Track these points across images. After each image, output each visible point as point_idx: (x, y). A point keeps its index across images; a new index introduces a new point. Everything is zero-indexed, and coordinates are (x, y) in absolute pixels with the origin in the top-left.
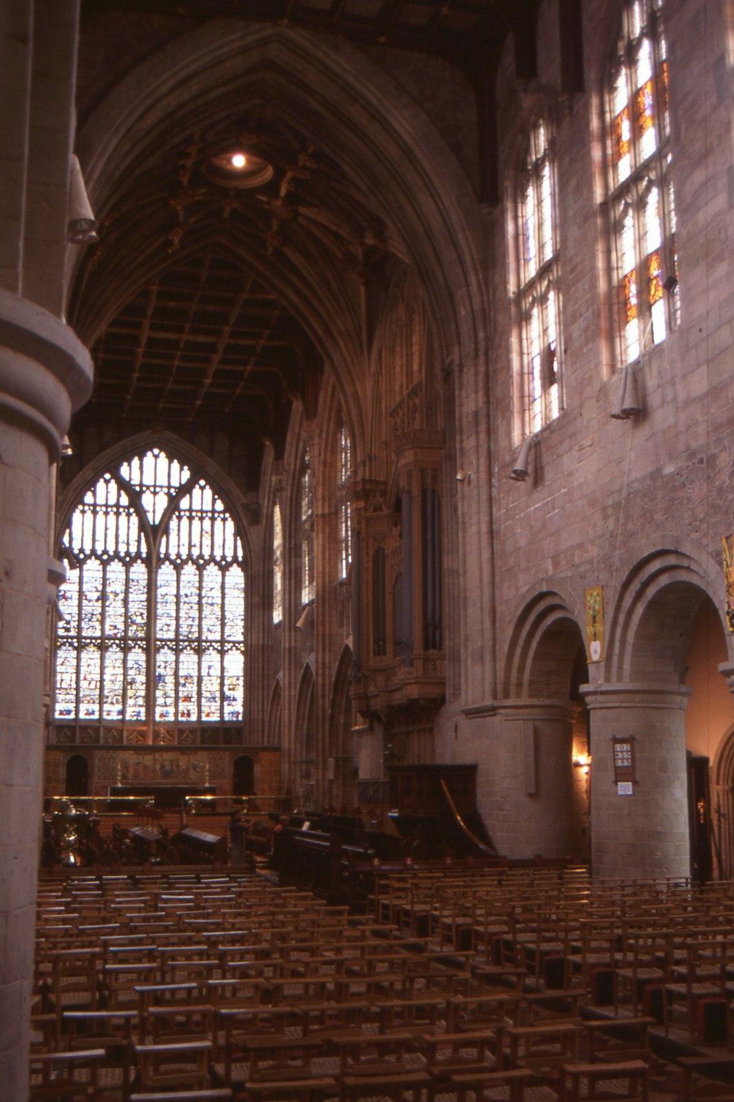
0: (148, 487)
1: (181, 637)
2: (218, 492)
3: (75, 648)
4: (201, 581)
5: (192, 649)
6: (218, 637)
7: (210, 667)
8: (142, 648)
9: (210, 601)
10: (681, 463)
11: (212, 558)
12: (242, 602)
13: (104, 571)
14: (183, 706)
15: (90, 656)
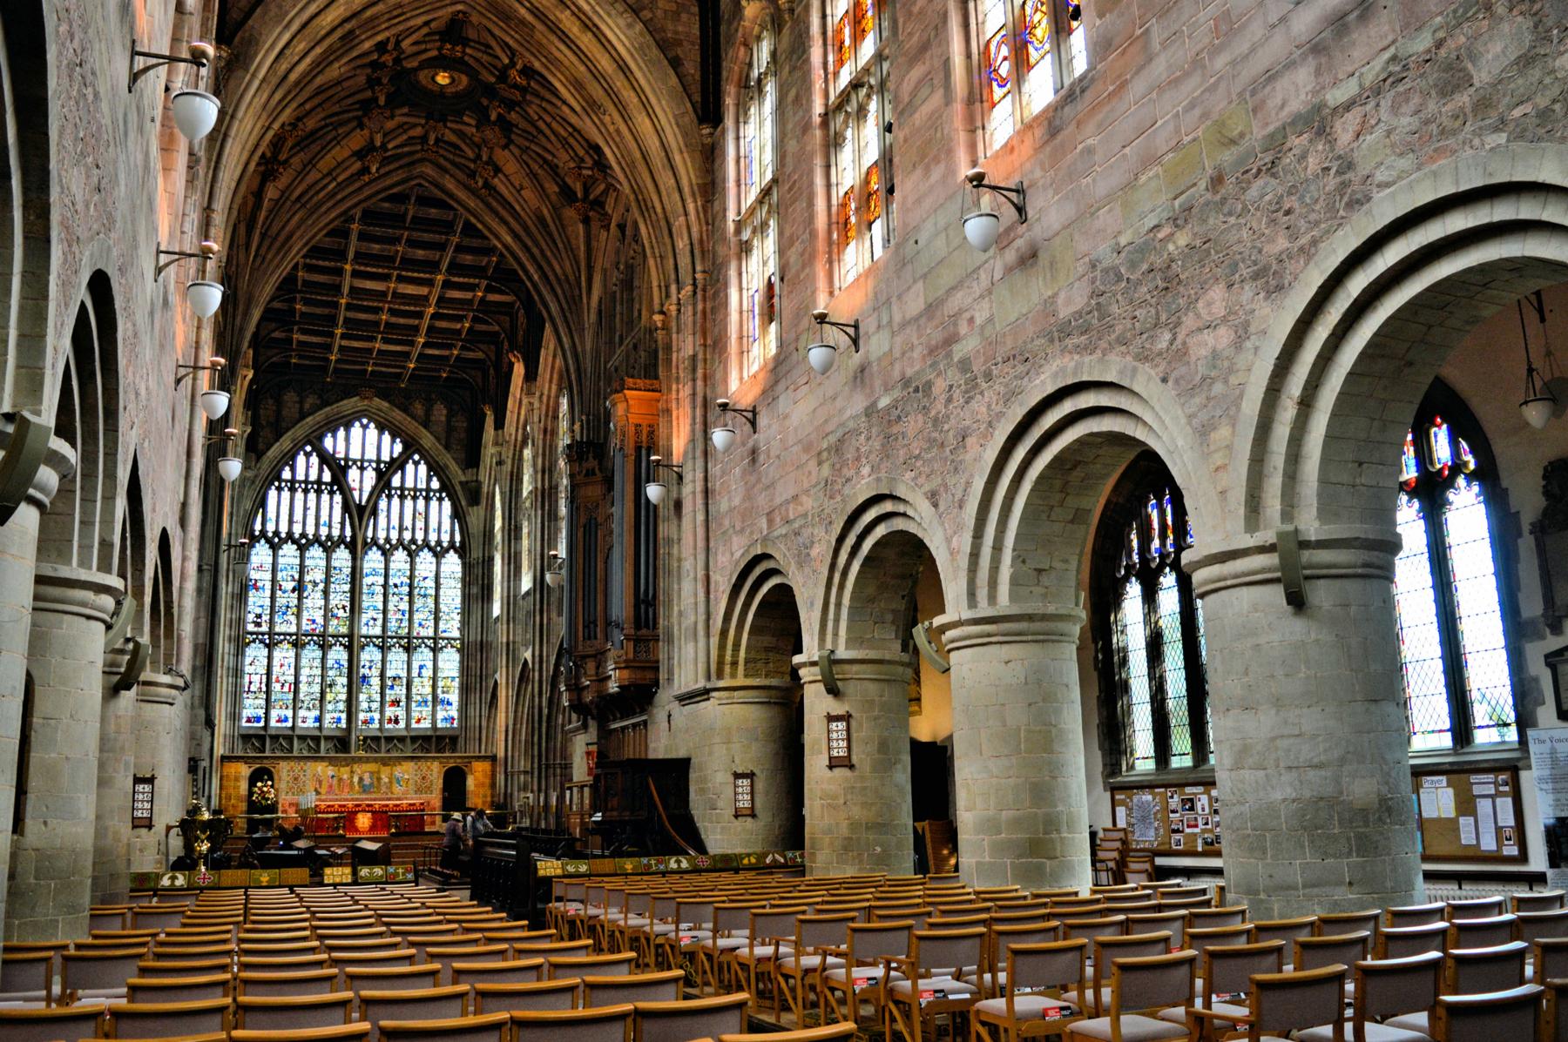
0: (355, 462)
2: (434, 469)
3: (268, 646)
4: (412, 569)
5: (400, 646)
6: (431, 633)
7: (421, 667)
9: (422, 592)
10: (897, 393)
11: (426, 544)
12: (459, 593)
13: (302, 558)
14: (390, 712)
15: (284, 654)
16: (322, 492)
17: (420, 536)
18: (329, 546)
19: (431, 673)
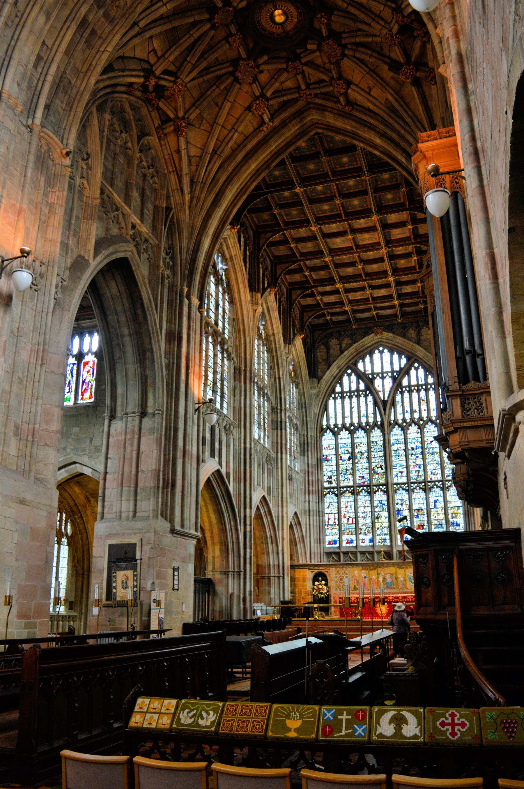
0: (378, 374)
1: (412, 481)
3: (337, 495)
4: (422, 437)
5: (420, 488)
6: (439, 477)
7: (435, 501)
8: (383, 491)
9: (431, 451)
13: (352, 438)
15: (347, 500)
16: (360, 396)
17: (424, 415)
18: (368, 429)
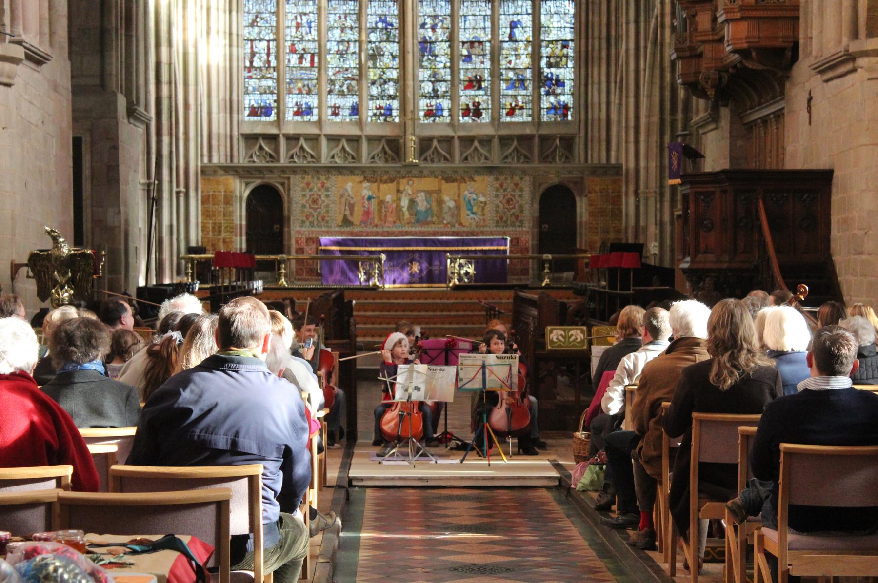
7: (513, 25)
15: (301, 9)
19: (529, 34)
